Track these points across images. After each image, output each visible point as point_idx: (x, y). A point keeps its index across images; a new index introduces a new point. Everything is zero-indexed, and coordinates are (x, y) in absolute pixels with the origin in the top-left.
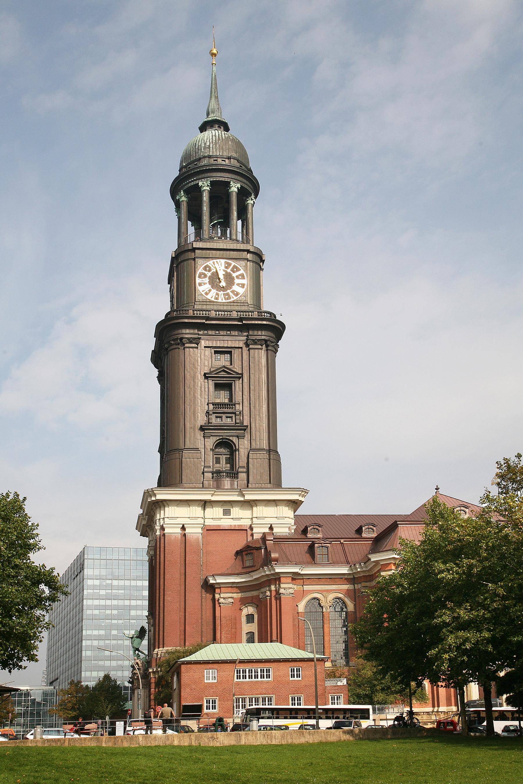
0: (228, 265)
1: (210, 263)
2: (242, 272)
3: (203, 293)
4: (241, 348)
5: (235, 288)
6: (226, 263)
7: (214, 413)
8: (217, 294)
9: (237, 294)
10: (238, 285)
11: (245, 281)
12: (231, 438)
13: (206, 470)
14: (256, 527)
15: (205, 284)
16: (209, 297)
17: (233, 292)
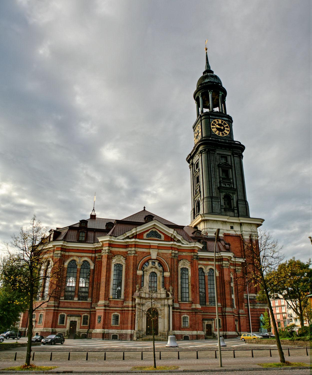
0: (222, 122)
1: (216, 120)
2: (227, 125)
3: (214, 132)
4: (230, 156)
5: (225, 131)
6: (221, 121)
7: (223, 182)
8: (219, 133)
9: (226, 134)
10: (226, 130)
11: (229, 129)
12: (230, 194)
13: (222, 207)
14: (245, 236)
15: (214, 128)
16: (216, 133)
17: (225, 132)
